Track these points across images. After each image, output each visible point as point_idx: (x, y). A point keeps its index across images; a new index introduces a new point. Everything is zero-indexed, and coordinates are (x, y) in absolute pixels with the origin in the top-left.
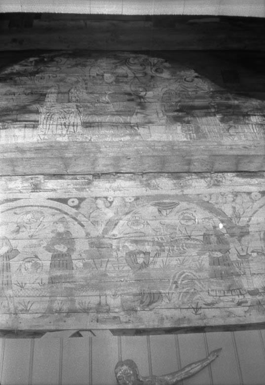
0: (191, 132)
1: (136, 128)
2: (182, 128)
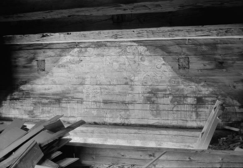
1: (128, 105)
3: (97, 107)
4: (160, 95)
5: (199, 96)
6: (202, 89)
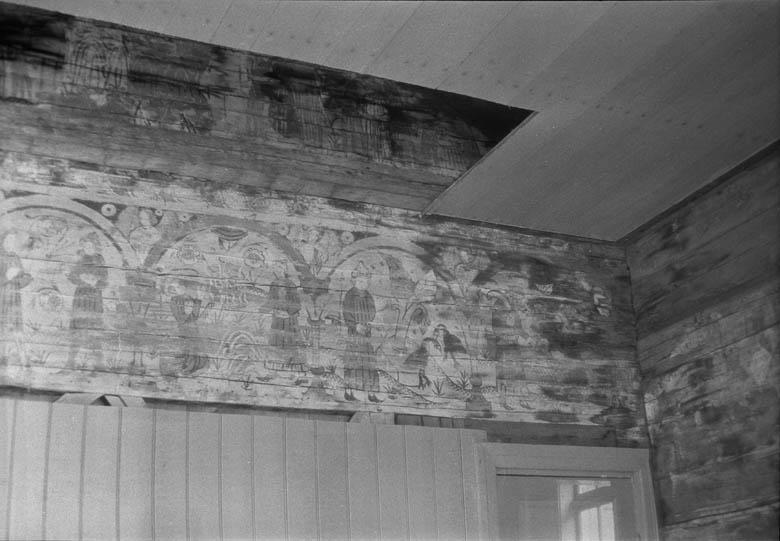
0: (281, 118)
1: (206, 95)
2: (270, 108)
3: (107, 87)
4: (298, 87)
5: (394, 104)
6: (400, 91)
